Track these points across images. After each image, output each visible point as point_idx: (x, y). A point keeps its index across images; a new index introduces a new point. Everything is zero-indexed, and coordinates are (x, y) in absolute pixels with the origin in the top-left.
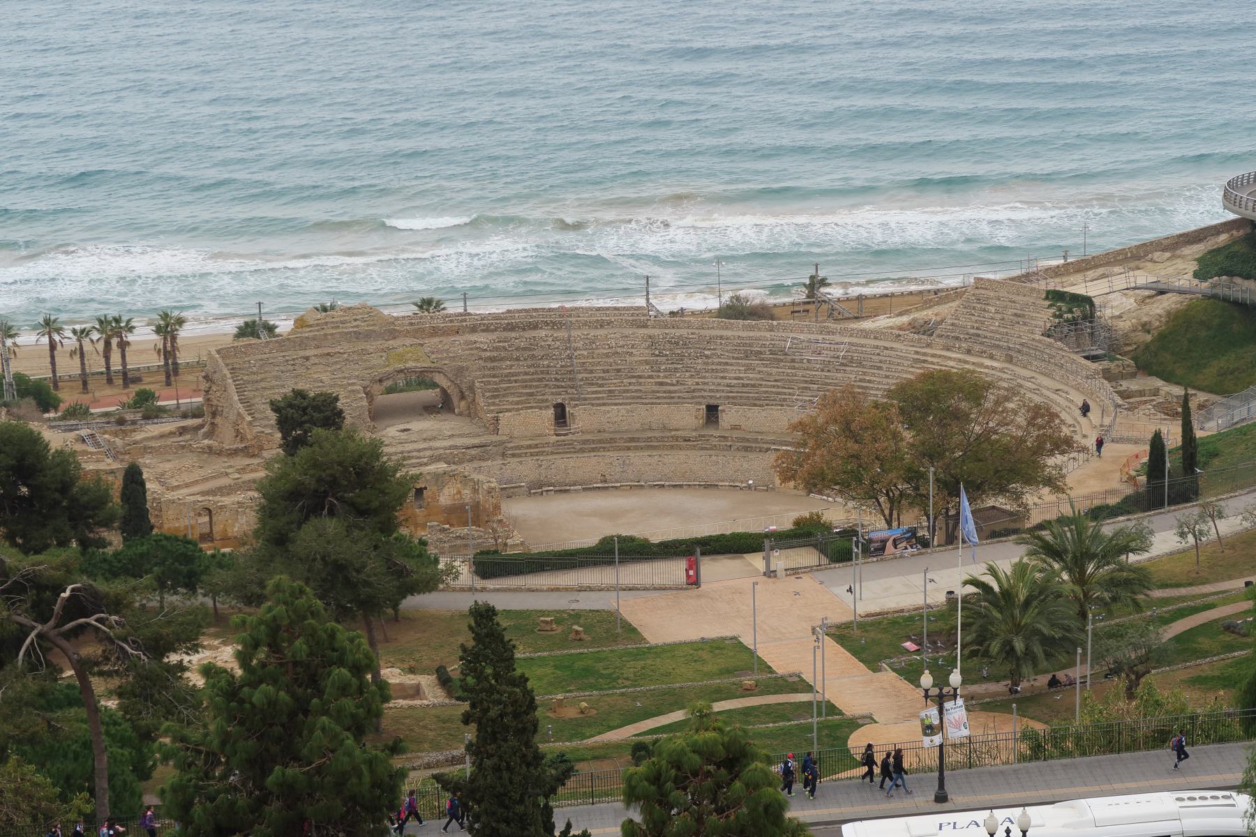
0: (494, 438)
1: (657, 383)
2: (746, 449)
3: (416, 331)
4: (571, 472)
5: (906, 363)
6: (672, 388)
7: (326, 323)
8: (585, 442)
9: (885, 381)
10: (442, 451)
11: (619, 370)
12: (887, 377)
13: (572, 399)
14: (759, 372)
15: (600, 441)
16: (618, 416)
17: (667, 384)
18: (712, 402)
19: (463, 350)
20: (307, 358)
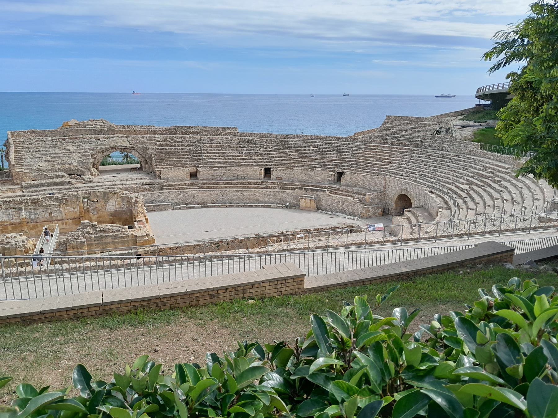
0: (159, 181)
1: (241, 159)
2: (285, 188)
3: (126, 131)
4: (196, 198)
5: (361, 150)
6: (248, 161)
7: (79, 125)
8: (204, 184)
9: (352, 157)
11: (224, 153)
12: (352, 156)
13: (199, 164)
14: (290, 155)
15: (212, 184)
16: (221, 171)
18: (267, 167)
19: (148, 140)
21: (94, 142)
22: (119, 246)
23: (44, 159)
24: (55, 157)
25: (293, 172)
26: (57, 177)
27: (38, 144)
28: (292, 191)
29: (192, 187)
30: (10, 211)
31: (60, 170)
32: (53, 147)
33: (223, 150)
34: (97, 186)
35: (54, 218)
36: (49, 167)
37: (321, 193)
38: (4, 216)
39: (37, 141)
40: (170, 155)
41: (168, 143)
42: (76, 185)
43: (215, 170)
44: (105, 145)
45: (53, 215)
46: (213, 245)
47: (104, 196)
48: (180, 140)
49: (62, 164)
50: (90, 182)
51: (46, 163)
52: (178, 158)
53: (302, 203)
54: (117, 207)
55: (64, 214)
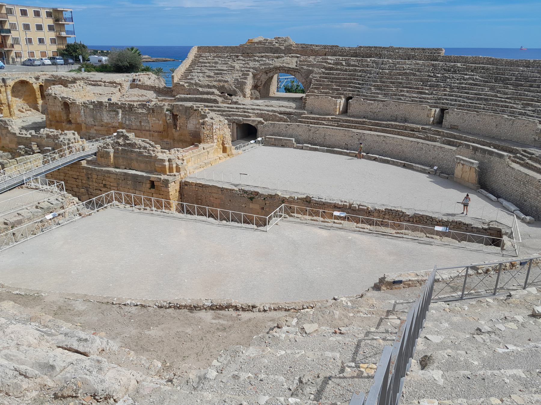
10: (263, 112)
17: (425, 93)
20: (237, 56)
21: (262, 60)
22: (143, 166)
23: (207, 74)
24: (218, 74)
25: (478, 118)
26: (208, 93)
27: (213, 59)
28: (454, 148)
29: (331, 123)
30: (112, 113)
31: (214, 87)
32: (224, 64)
33: (401, 79)
34: (237, 108)
36: (207, 83)
37: (497, 159)
38: (108, 118)
39: (214, 57)
40: (332, 82)
41: (339, 67)
42: (220, 105)
43: (369, 104)
44: (271, 64)
46: (245, 195)
47: (186, 111)
48: (356, 63)
49: (220, 81)
50: (236, 103)
52: (339, 86)
53: (458, 171)
55: (151, 125)
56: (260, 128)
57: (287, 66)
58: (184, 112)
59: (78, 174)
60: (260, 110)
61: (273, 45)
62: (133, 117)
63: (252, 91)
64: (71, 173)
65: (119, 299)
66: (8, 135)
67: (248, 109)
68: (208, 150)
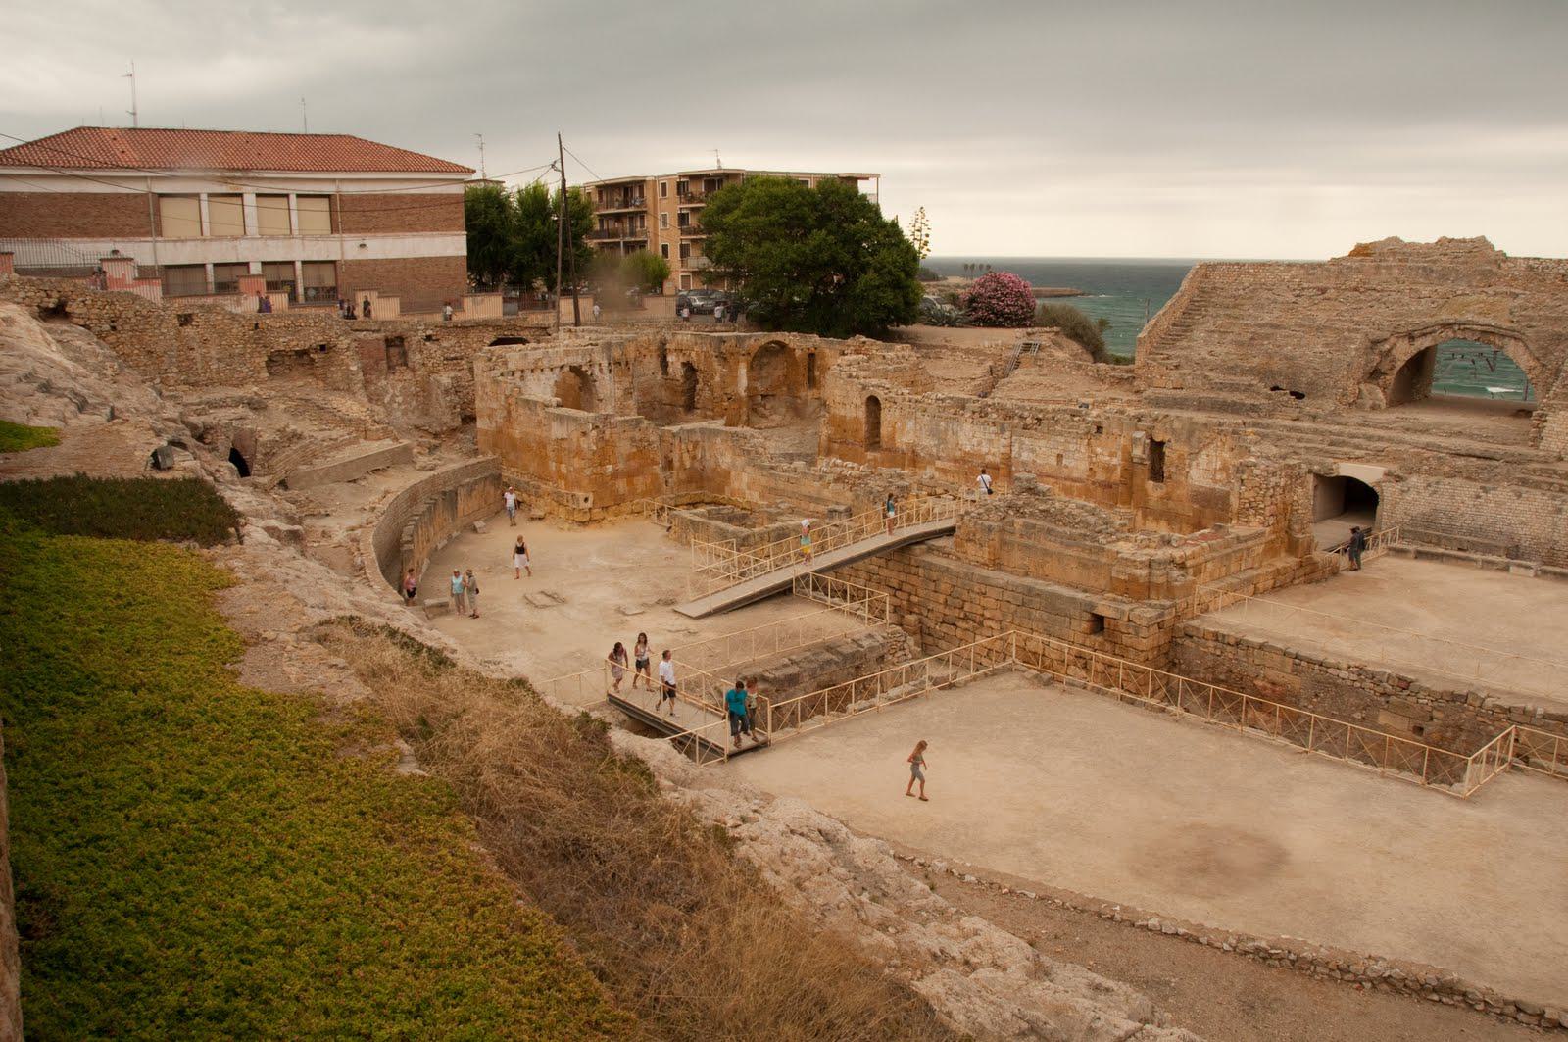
10: (1402, 448)
20: (1323, 291)
35: (1065, 472)
45: (1064, 462)
47: (1191, 434)
51: (1232, 349)
54: (1218, 477)
56: (1388, 493)
57: (1481, 320)
58: (1183, 438)
59: (902, 577)
60: (1389, 440)
61: (1434, 262)
62: (1042, 443)
63: (1362, 386)
64: (884, 573)
65: (1125, 909)
66: (749, 469)
67: (1353, 436)
68: (1250, 543)
